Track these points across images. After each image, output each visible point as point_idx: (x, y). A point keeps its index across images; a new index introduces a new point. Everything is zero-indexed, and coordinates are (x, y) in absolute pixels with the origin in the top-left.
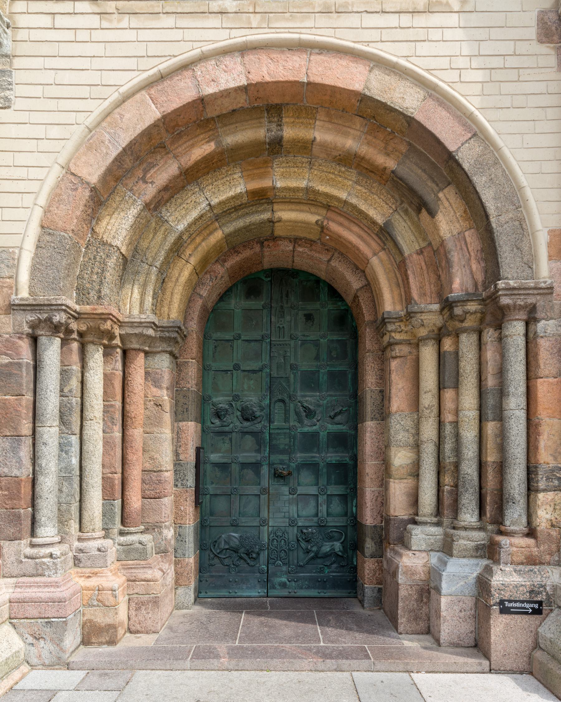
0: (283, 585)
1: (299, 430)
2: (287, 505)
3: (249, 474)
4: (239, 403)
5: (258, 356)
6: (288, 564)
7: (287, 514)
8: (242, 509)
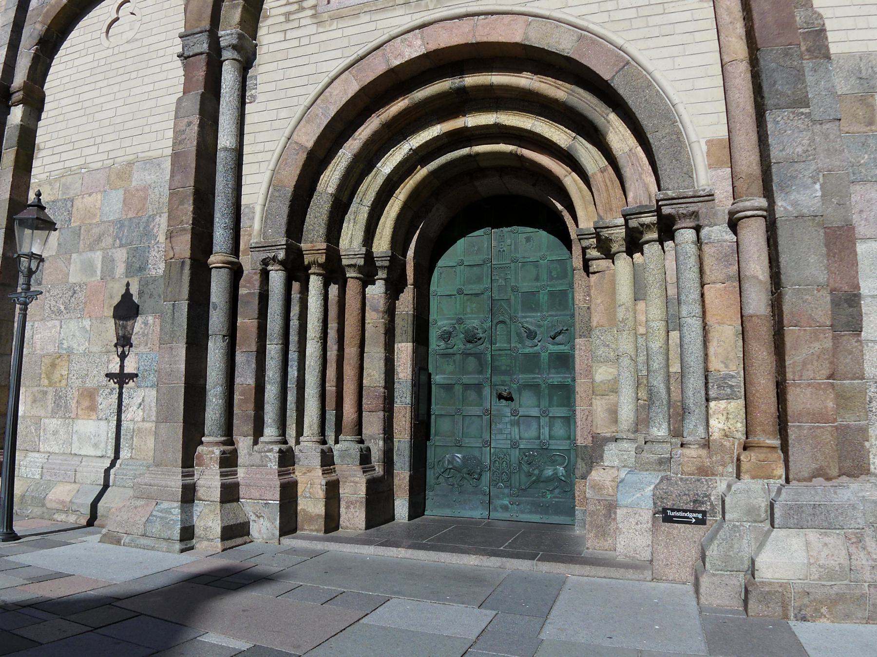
0: (505, 508)
1: (520, 352)
2: (509, 426)
3: (472, 395)
4: (462, 326)
5: (479, 279)
6: (510, 487)
7: (509, 436)
8: (465, 429)
